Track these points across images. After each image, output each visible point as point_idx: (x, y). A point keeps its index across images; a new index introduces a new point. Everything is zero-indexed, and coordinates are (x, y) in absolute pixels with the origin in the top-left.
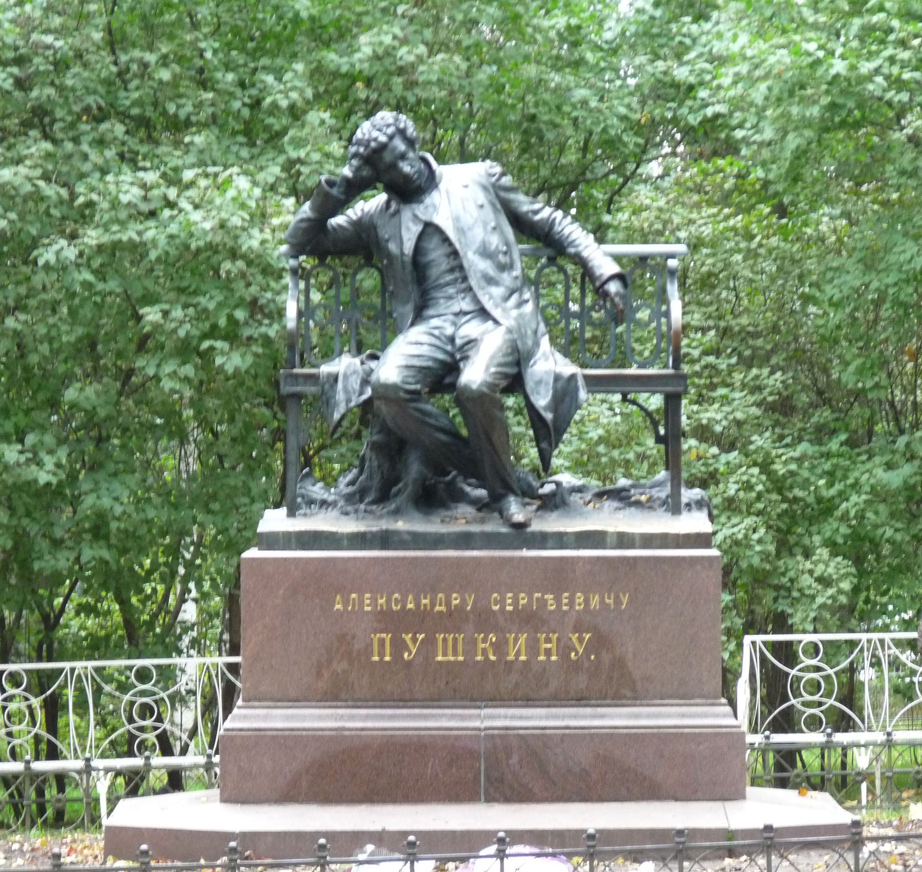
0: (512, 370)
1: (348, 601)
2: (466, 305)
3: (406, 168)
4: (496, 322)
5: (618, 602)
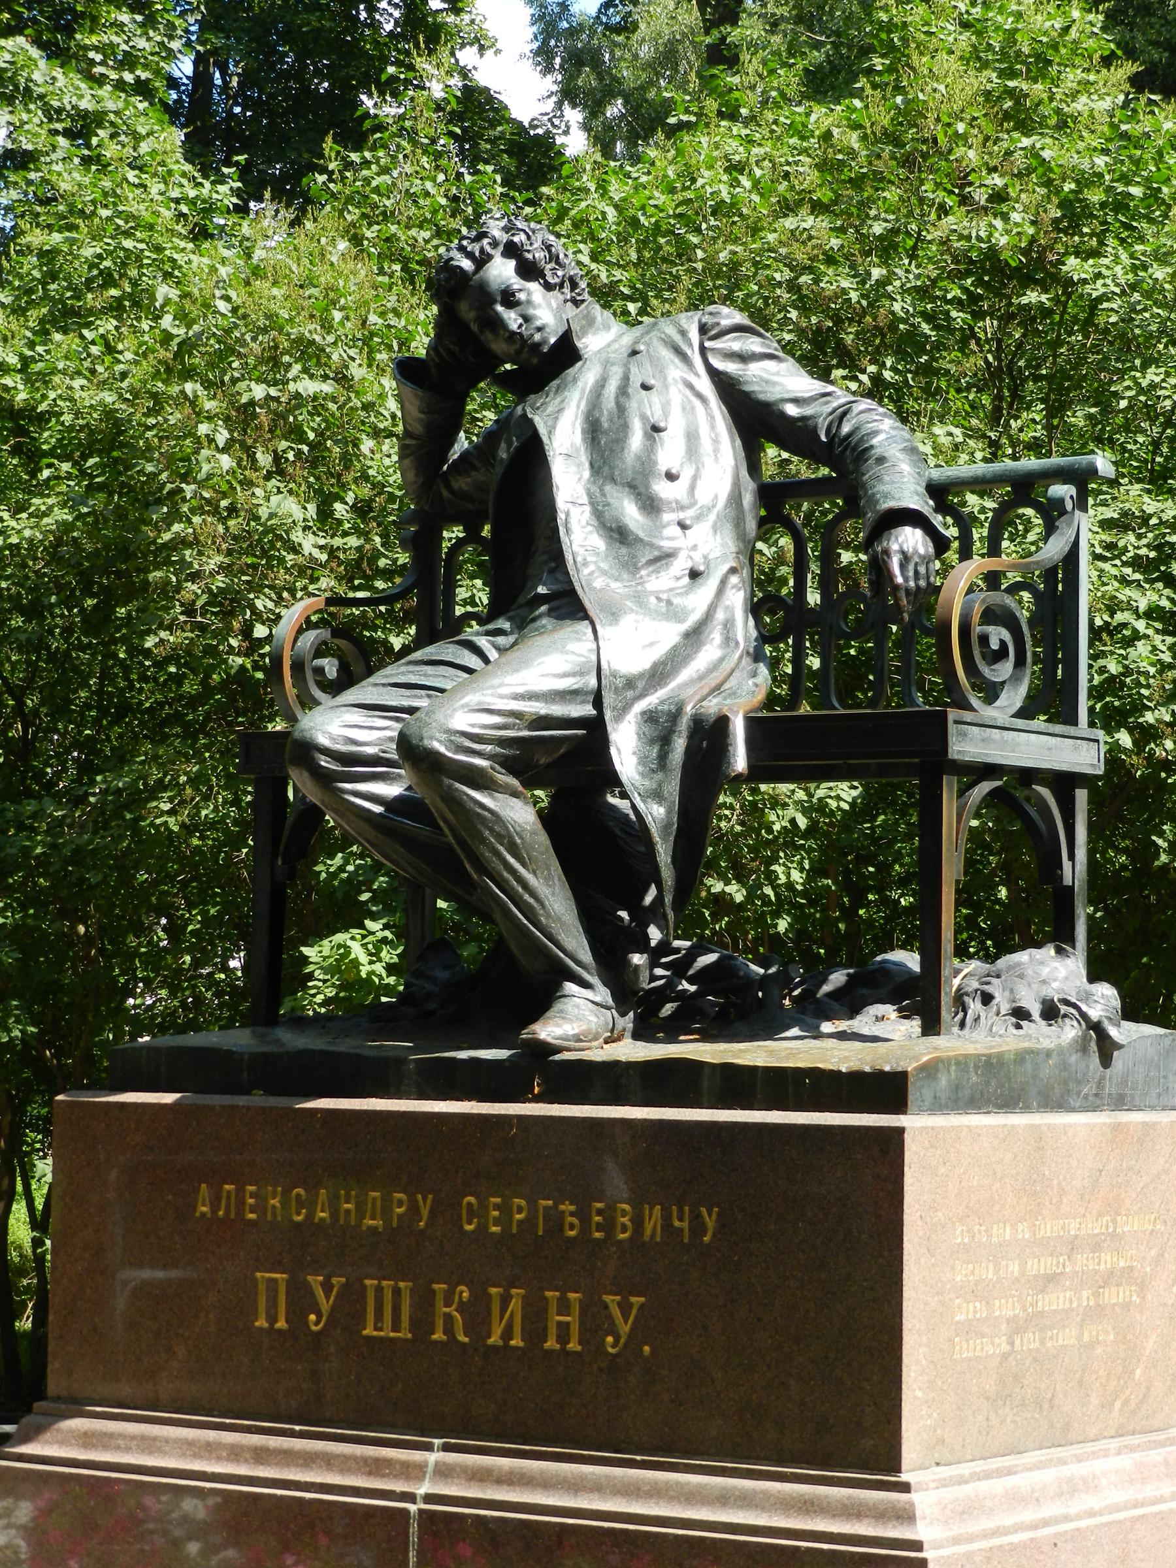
0: (588, 710)
1: (219, 1199)
3: (512, 319)
4: (586, 617)
5: (698, 1227)
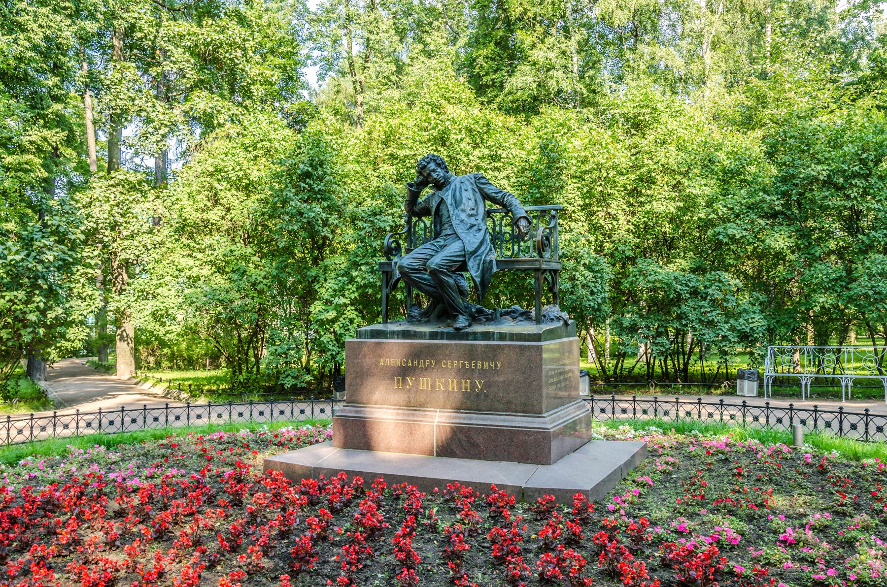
2: (449, 232)
5: (496, 366)
